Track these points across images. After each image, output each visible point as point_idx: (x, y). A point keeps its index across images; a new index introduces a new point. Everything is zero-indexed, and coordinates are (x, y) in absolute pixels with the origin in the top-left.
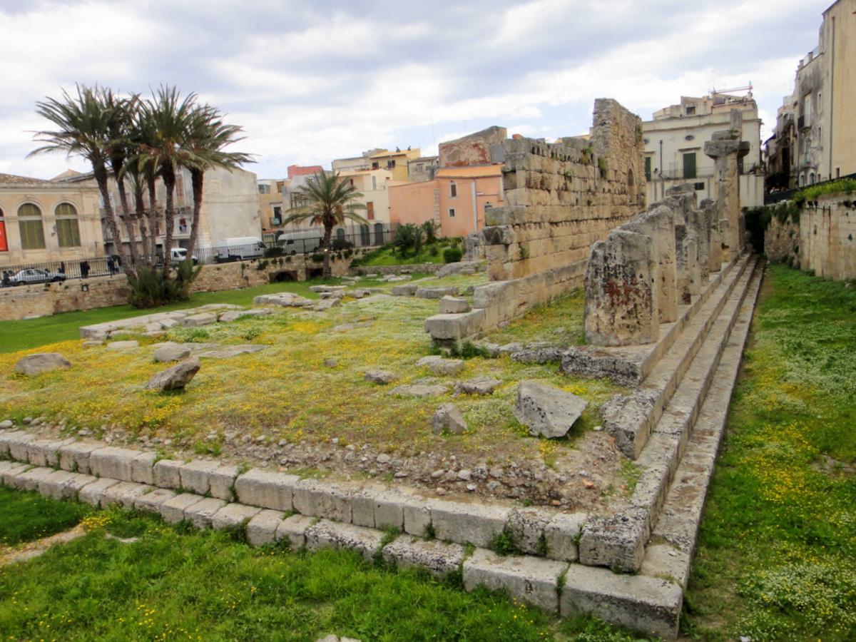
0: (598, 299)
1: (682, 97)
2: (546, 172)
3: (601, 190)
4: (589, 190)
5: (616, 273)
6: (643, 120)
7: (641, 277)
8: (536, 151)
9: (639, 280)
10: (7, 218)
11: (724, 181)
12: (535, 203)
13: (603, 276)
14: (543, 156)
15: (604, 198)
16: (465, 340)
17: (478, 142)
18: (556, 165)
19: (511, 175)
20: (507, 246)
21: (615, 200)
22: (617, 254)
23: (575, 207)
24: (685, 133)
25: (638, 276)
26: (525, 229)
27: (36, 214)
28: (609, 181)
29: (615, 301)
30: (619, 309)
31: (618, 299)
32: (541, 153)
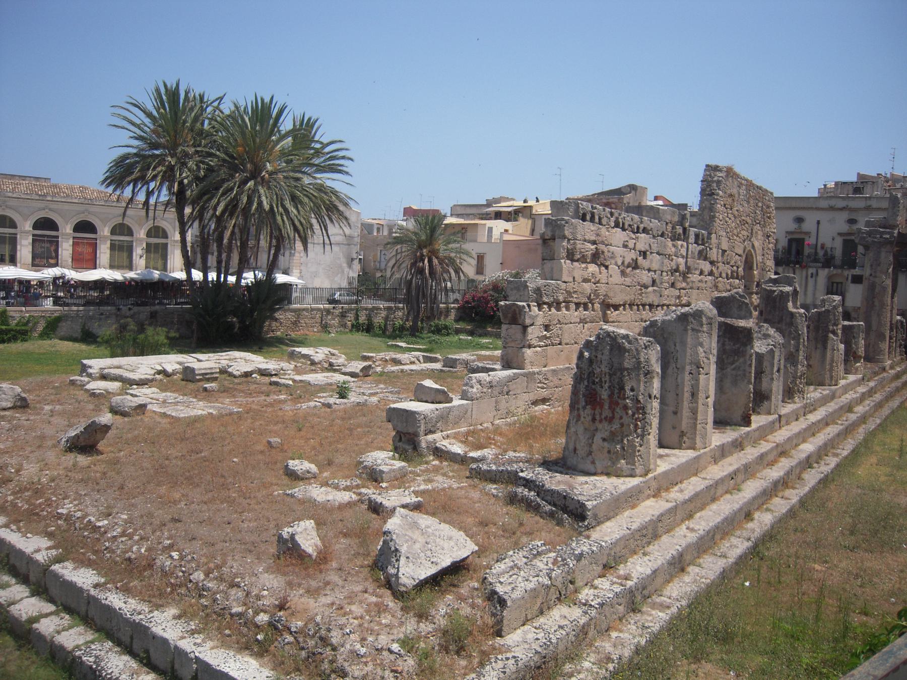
0: (578, 409)
1: (858, 174)
2: (603, 243)
3: (698, 272)
4: (677, 270)
5: (601, 380)
6: (775, 195)
7: (632, 390)
8: (588, 218)
9: (629, 393)
10: (63, 234)
11: (875, 277)
12: (579, 279)
13: (586, 383)
14: (600, 223)
15: (700, 281)
16: (430, 437)
17: (611, 200)
18: (619, 236)
19: (551, 243)
20: (525, 328)
21: (719, 285)
22: (604, 357)
23: (651, 289)
24: (845, 216)
25: (627, 388)
26: (558, 309)
27: (127, 235)
28: (712, 263)
29: (598, 417)
30: (600, 426)
31: (601, 414)
32: (597, 220)
